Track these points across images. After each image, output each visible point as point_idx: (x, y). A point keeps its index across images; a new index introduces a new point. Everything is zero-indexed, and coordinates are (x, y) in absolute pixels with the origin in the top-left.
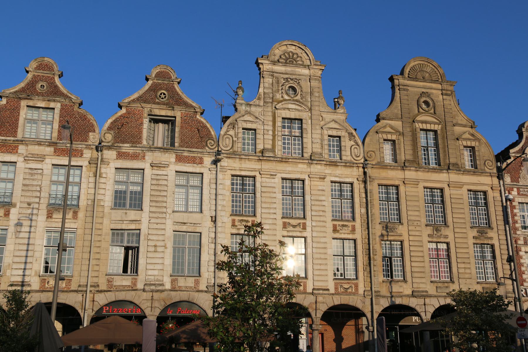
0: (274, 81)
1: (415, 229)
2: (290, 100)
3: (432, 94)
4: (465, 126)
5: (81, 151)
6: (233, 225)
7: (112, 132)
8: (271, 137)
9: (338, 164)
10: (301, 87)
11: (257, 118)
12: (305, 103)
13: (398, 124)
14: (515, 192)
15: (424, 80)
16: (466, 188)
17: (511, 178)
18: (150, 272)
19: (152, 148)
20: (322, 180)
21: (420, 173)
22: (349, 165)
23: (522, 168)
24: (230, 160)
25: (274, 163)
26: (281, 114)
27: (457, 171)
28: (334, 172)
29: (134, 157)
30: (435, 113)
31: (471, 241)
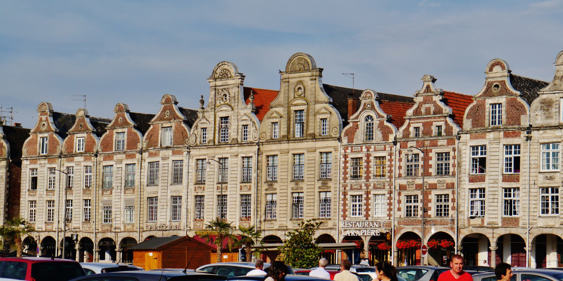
0: (216, 93)
1: (283, 185)
2: (224, 104)
3: (304, 81)
4: (322, 103)
5: (135, 155)
6: (195, 190)
7: (147, 141)
8: (213, 132)
9: (244, 145)
10: (229, 93)
11: (207, 120)
12: (231, 104)
13: (280, 110)
14: (349, 151)
15: (300, 71)
16: (318, 151)
17: (348, 139)
18: (162, 220)
19: (162, 148)
20: (236, 157)
21: (290, 144)
22: (251, 144)
23: (357, 130)
24: (195, 150)
25: (214, 149)
26: (218, 115)
27: (311, 139)
28: (243, 151)
29: (156, 155)
30: (304, 96)
31: (317, 190)
